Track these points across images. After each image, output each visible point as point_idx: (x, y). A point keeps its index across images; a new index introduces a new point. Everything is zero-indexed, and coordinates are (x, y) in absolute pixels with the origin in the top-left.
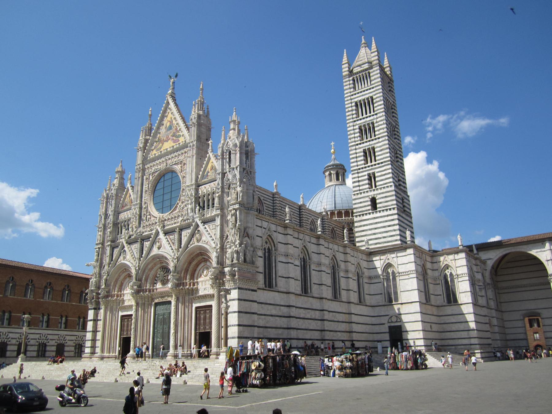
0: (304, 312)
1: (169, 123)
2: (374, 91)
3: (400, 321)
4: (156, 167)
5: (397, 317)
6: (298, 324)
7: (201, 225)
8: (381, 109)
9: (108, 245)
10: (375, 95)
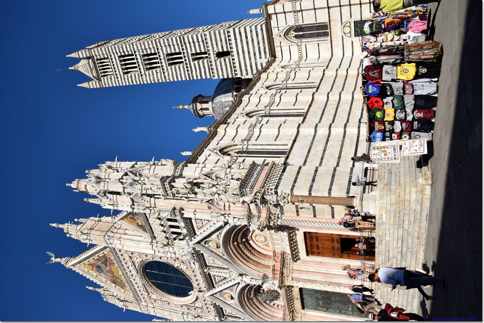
0: (326, 116)
1: (94, 268)
2: (114, 54)
3: (350, 22)
4: (142, 289)
5: (344, 27)
6: (341, 122)
7: (198, 238)
8: (130, 47)
10: (117, 53)
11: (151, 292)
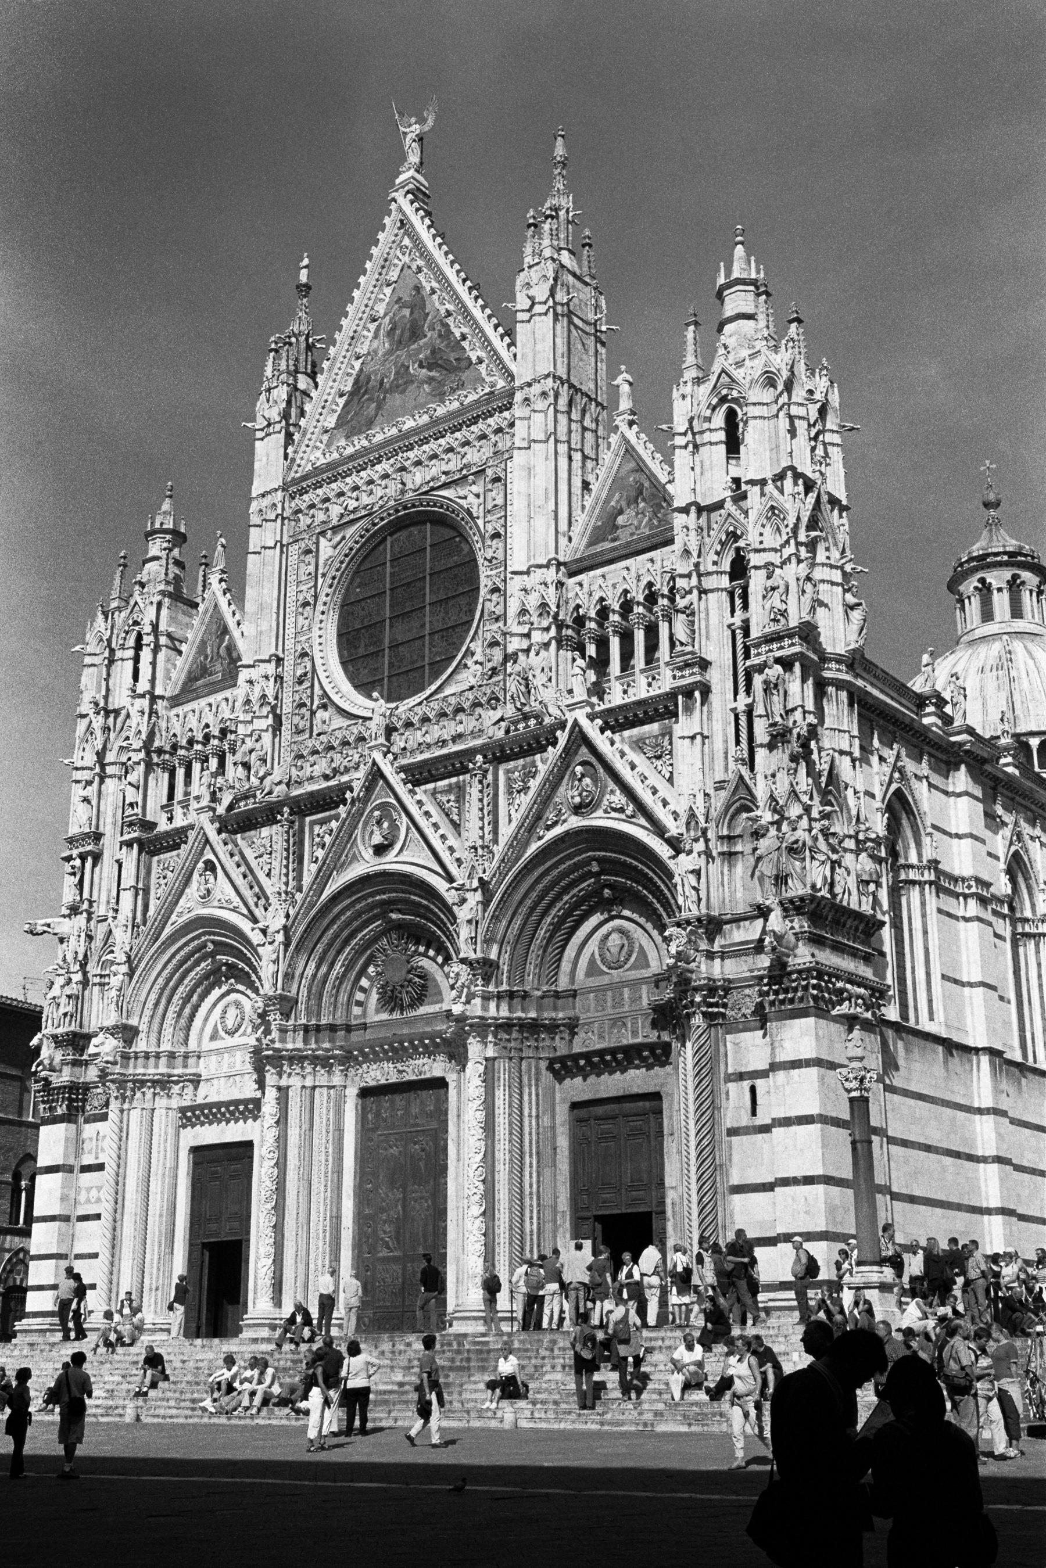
1: (407, 312)
4: (352, 504)
7: (601, 741)
9: (129, 844)
11: (344, 538)
